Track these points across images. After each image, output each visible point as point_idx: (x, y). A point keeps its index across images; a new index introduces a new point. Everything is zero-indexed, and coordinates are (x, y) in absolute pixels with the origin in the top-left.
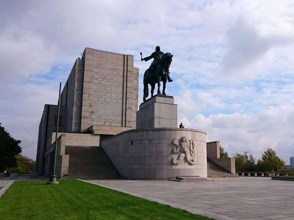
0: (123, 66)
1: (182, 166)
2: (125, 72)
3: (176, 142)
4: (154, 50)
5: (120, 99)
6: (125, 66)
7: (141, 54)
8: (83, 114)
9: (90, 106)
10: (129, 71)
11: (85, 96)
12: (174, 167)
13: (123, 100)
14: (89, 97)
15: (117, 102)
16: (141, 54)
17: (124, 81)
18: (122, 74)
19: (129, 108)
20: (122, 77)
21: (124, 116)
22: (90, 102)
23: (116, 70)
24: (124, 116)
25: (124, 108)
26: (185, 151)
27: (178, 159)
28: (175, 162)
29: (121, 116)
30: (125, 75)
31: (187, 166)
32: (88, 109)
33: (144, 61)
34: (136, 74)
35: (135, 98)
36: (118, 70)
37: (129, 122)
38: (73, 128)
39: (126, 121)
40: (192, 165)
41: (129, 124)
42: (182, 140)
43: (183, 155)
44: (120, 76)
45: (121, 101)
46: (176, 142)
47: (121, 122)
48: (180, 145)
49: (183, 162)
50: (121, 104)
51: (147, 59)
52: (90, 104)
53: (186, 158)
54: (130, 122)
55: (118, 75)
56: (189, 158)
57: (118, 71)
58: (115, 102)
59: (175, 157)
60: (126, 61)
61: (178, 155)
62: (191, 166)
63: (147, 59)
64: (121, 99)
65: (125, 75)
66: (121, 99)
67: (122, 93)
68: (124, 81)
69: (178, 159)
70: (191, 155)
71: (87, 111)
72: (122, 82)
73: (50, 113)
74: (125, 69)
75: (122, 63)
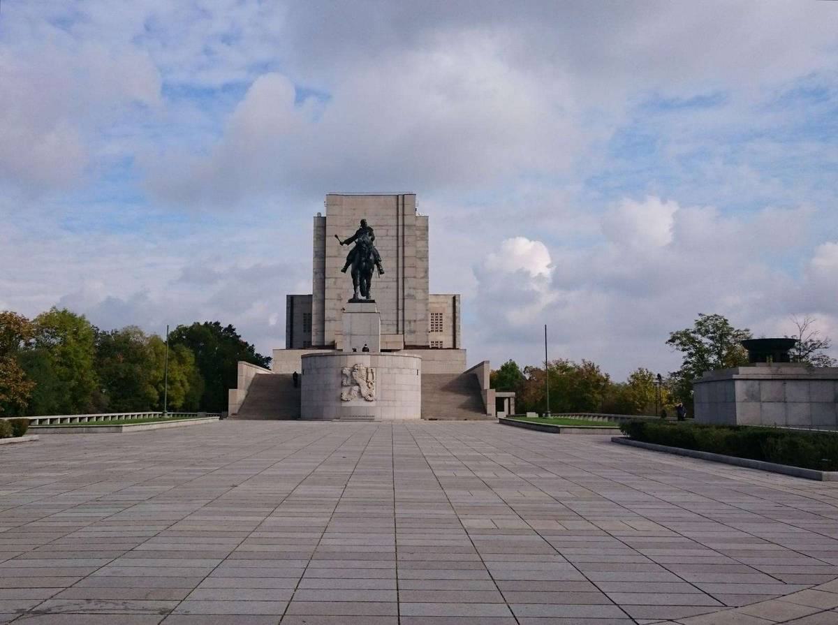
0: (395, 217)
1: (355, 403)
2: (400, 228)
3: (347, 371)
4: (358, 226)
5: (392, 280)
6: (400, 217)
7: (336, 236)
8: (328, 314)
9: (338, 300)
10: (407, 226)
11: (328, 283)
12: (344, 404)
13: (398, 281)
14: (335, 283)
15: (387, 288)
16: (336, 236)
17: (398, 247)
18: (393, 232)
19: (409, 295)
20: (395, 238)
21: (400, 312)
22: (338, 291)
23: (383, 228)
24: (400, 312)
25: (400, 297)
26: (358, 382)
27: (349, 393)
28: (344, 398)
29: (395, 311)
30: (400, 234)
31: (363, 403)
32: (335, 305)
33: (344, 245)
34: (422, 228)
35: (422, 275)
36: (386, 225)
37: (410, 322)
38: (315, 339)
39: (404, 320)
40: (372, 401)
41: (410, 326)
42: (353, 369)
43: (356, 388)
44: (391, 238)
45: (395, 284)
46: (347, 371)
47: (395, 323)
48: (351, 374)
49: (357, 398)
50: (395, 291)
51: (348, 242)
52: (339, 295)
53: (360, 392)
54: (412, 323)
55: (387, 235)
56: (365, 391)
57: (386, 228)
58: (384, 288)
59: (345, 391)
60: (400, 207)
61: (349, 388)
62: (369, 403)
63: (348, 242)
64: (395, 280)
65: (400, 234)
66: (393, 281)
67: (396, 269)
68: (398, 247)
69: (349, 393)
70: (369, 388)
71: (333, 309)
72: (395, 249)
73: (295, 311)
74: (400, 223)
75: (394, 212)
